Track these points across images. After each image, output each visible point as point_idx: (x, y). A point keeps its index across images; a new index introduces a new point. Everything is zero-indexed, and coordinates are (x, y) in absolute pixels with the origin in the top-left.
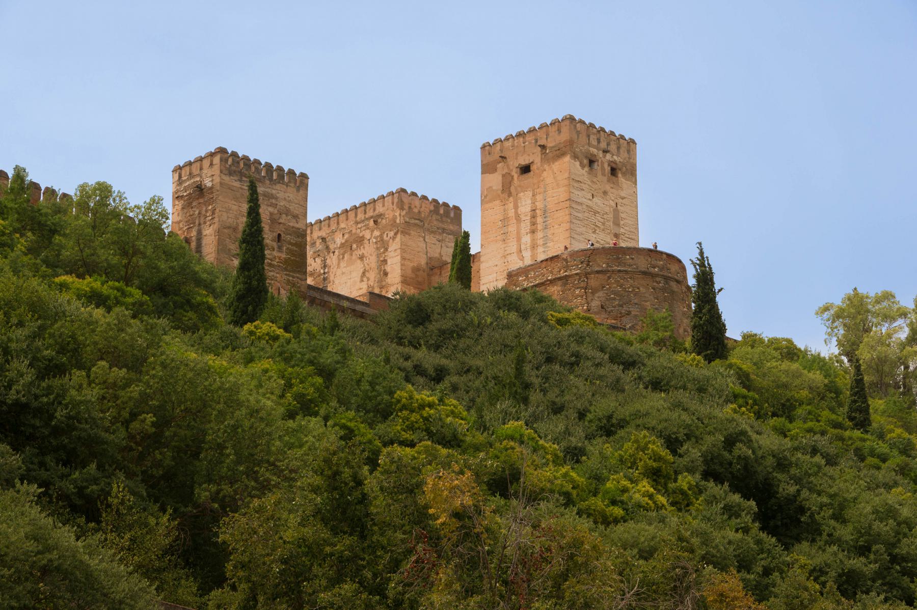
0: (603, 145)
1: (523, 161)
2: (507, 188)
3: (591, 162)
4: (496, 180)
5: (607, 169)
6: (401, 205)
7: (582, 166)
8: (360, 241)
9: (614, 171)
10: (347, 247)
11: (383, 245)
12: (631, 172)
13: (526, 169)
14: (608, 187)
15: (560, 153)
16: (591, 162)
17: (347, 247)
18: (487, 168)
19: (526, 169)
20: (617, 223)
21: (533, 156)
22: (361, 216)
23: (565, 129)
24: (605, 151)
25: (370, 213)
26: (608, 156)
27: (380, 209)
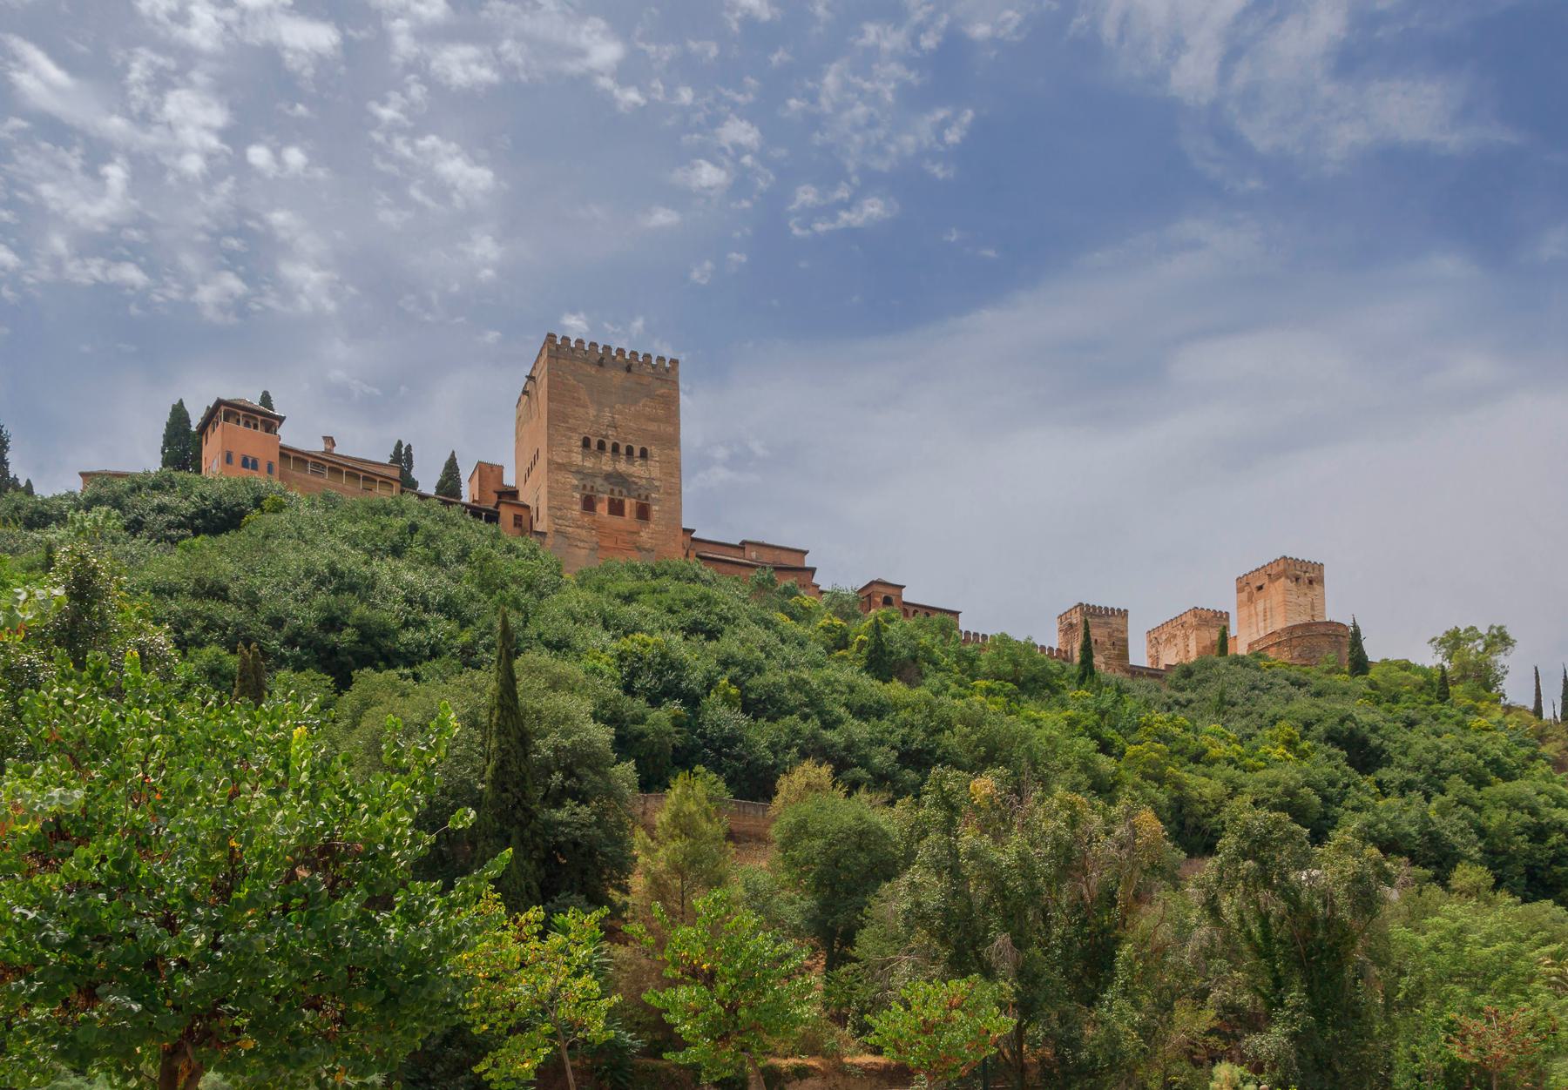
0: (1304, 569)
1: (1259, 584)
2: (1250, 599)
3: (1297, 579)
4: (1244, 595)
5: (1307, 581)
6: (1195, 616)
7: (1292, 582)
8: (1175, 636)
9: (1311, 582)
10: (1168, 640)
11: (1186, 637)
12: (1321, 581)
13: (1260, 588)
14: (1307, 591)
15: (1278, 576)
16: (1297, 579)
17: (1168, 640)
18: (1240, 590)
19: (1260, 588)
20: (1313, 609)
21: (1265, 580)
22: (1174, 624)
23: (1281, 563)
24: (1305, 572)
25: (1179, 622)
26: (1307, 575)
27: (1184, 619)
